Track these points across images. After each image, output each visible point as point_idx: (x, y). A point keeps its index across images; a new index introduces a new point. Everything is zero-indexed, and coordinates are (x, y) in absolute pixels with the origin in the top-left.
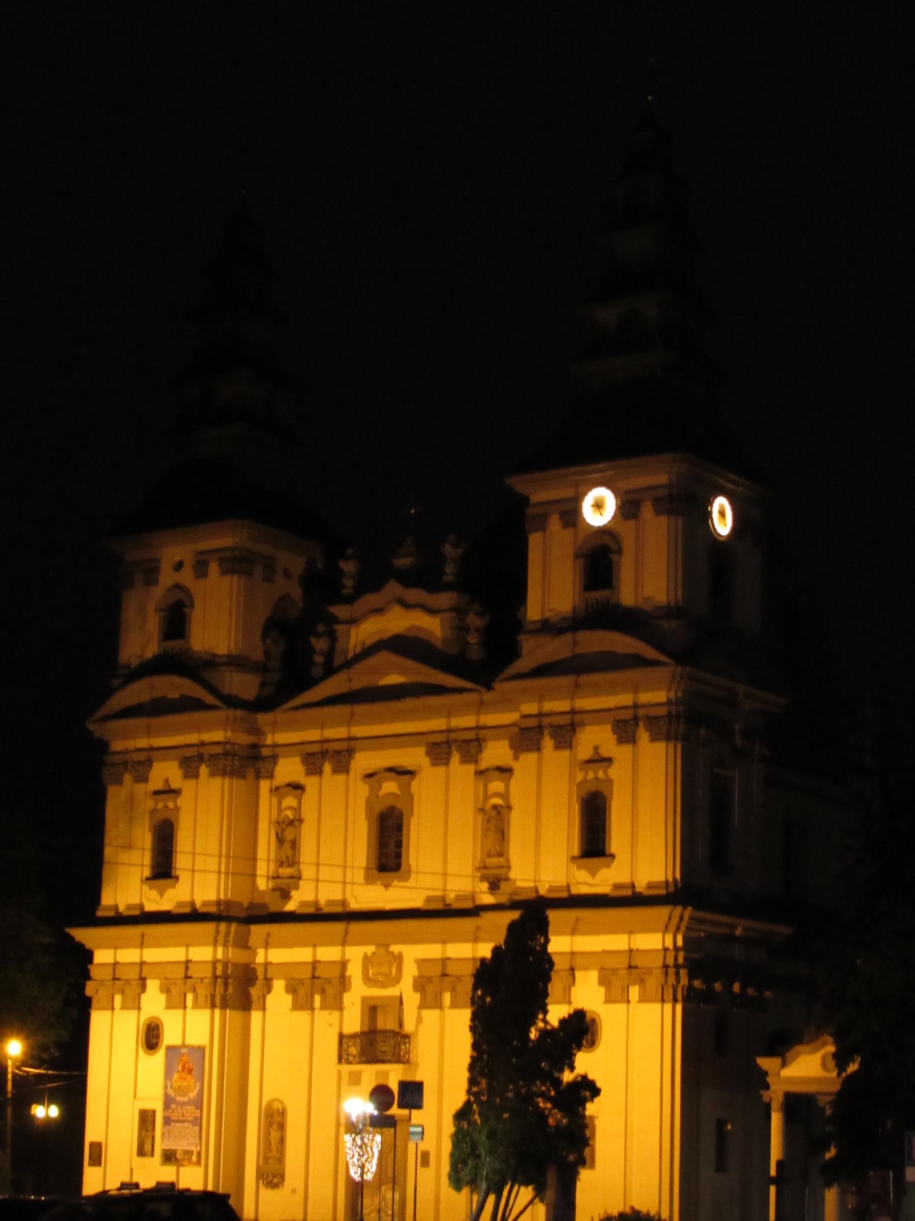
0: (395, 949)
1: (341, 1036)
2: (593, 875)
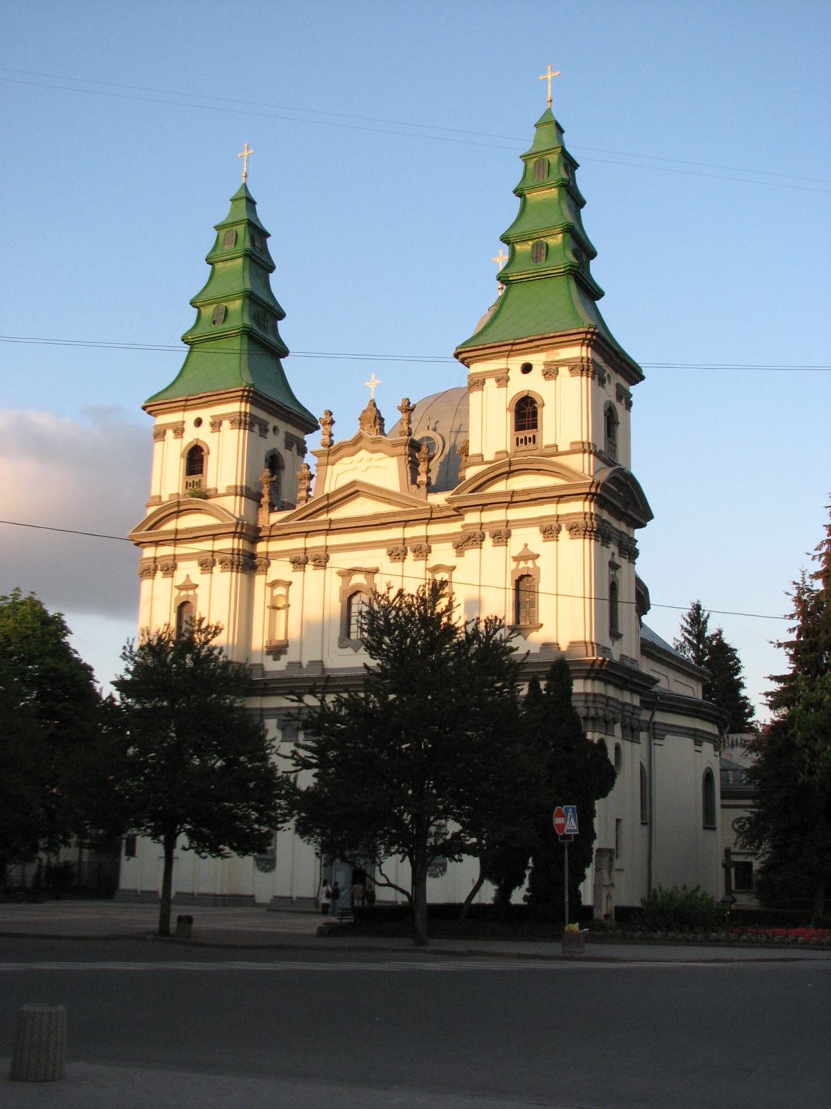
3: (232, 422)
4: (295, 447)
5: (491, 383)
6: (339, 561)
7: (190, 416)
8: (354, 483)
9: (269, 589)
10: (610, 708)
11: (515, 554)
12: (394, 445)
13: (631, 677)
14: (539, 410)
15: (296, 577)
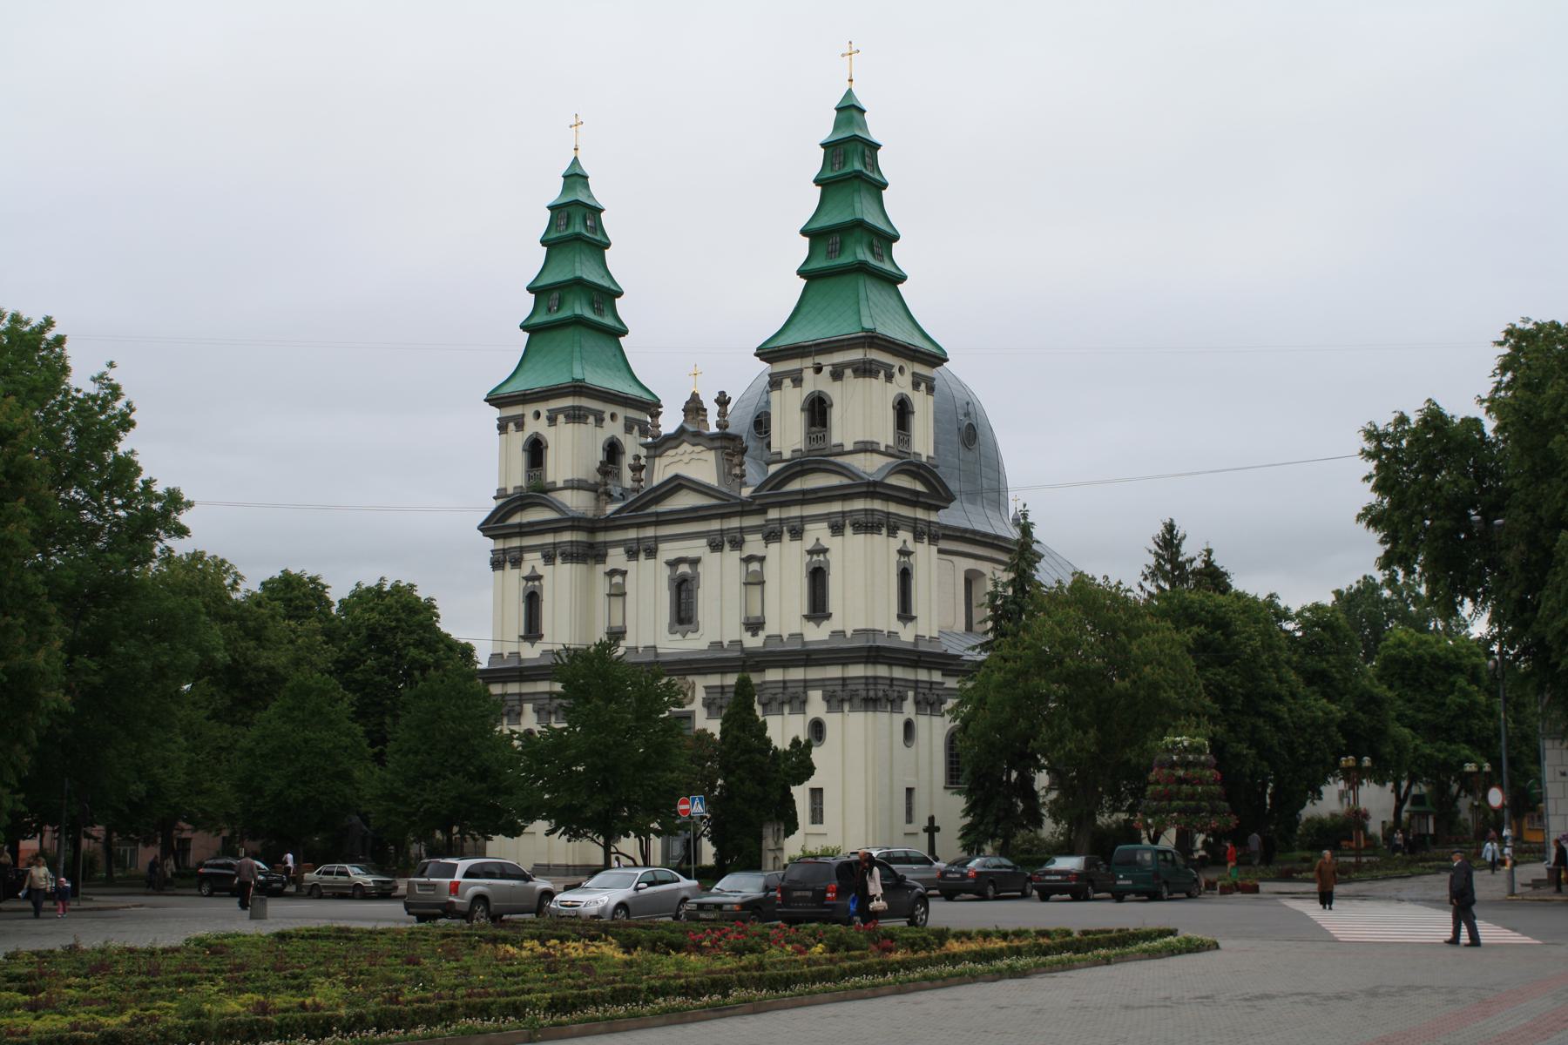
0: (690, 679)
2: (818, 626)
3: (566, 417)
4: (636, 428)
5: (787, 382)
6: (668, 551)
7: (528, 410)
8: (677, 477)
9: (607, 579)
10: (895, 688)
11: (808, 548)
12: (713, 437)
13: (920, 657)
14: (828, 410)
15: (631, 566)
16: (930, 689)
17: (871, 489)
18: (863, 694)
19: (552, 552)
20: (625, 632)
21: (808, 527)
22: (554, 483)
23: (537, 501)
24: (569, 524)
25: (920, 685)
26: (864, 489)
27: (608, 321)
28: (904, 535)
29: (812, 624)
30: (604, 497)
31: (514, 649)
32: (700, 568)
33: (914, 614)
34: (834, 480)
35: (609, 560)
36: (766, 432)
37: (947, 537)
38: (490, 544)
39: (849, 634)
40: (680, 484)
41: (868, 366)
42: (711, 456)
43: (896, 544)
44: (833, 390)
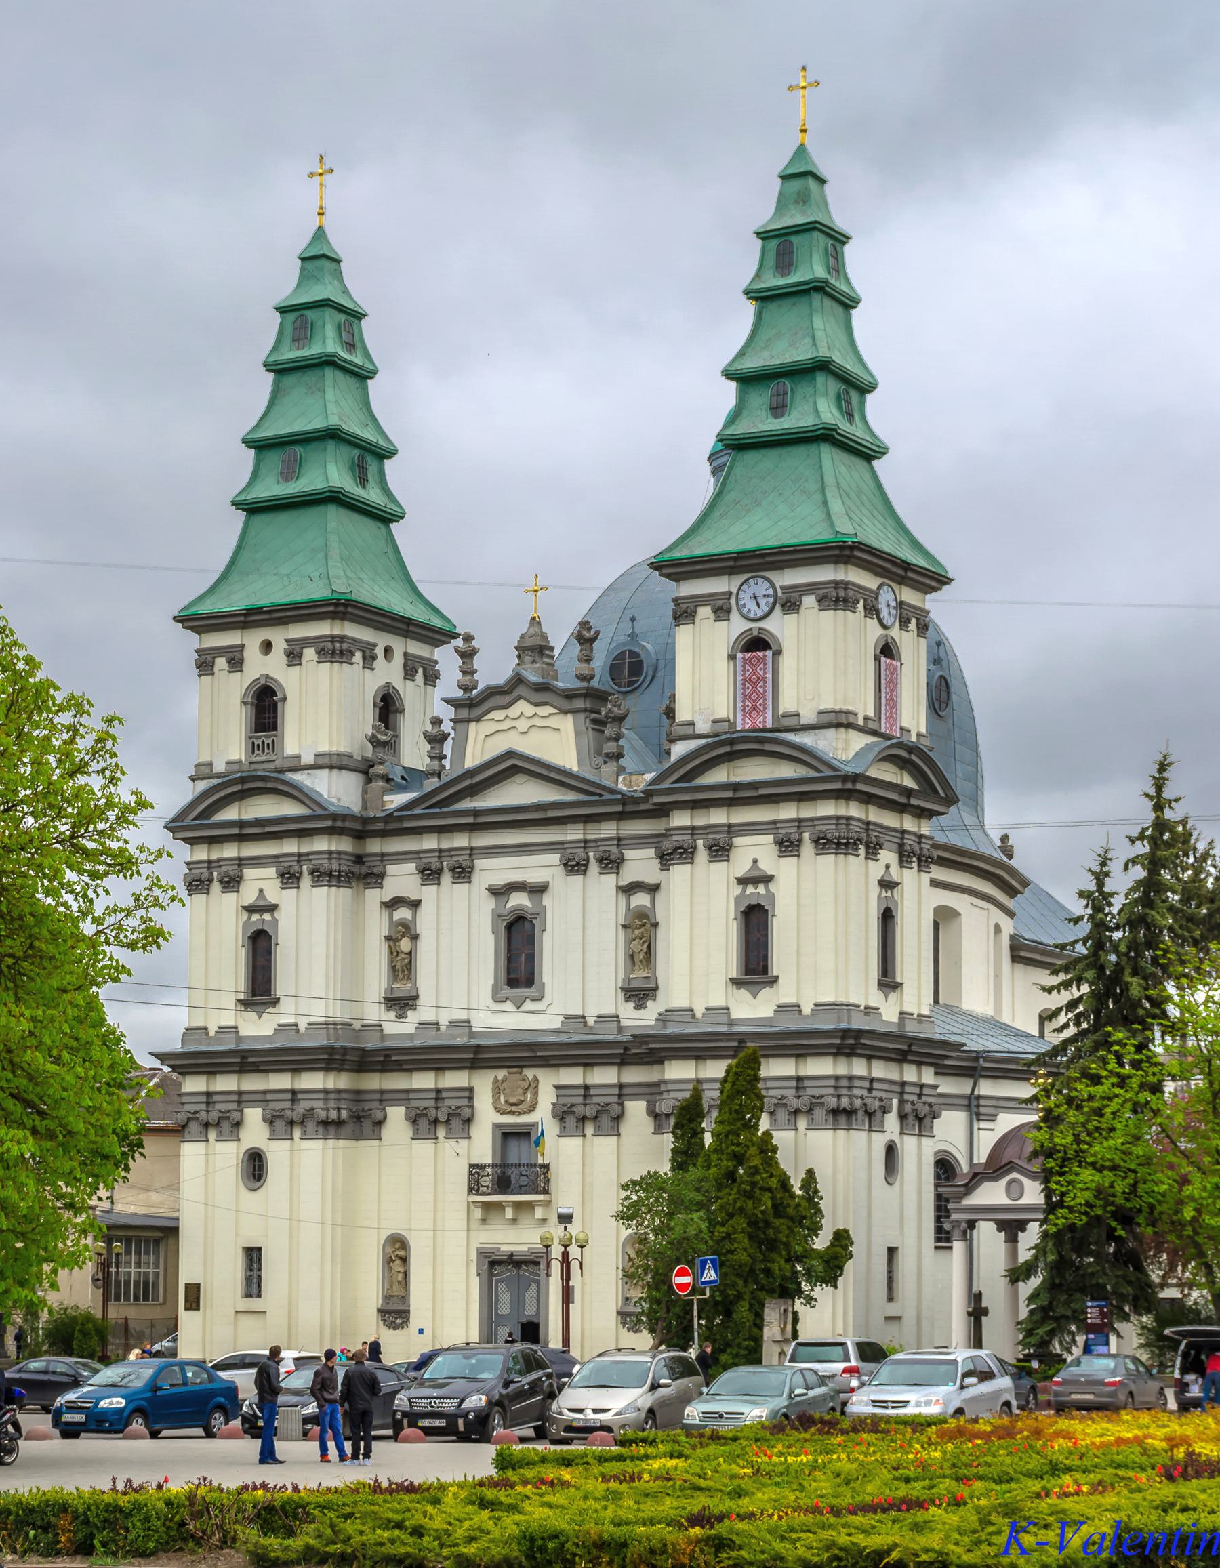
0: (529, 1073)
1: (471, 1166)
5: (705, 612)
6: (493, 871)
7: (252, 640)
8: (510, 754)
9: (386, 914)
11: (740, 873)
12: (569, 696)
13: (910, 1046)
15: (428, 894)
16: (920, 1095)
17: (849, 786)
18: (833, 1102)
19: (295, 868)
20: (417, 997)
21: (738, 841)
22: (298, 757)
23: (270, 785)
24: (329, 823)
25: (907, 1089)
26: (838, 786)
27: (373, 495)
28: (888, 856)
29: (744, 994)
30: (380, 784)
31: (228, 1019)
32: (547, 900)
33: (898, 980)
34: (786, 771)
35: (387, 882)
36: (630, 684)
37: (943, 862)
38: (183, 853)
39: (807, 1009)
40: (514, 766)
41: (842, 593)
42: (567, 724)
43: (876, 870)
44: (780, 626)
